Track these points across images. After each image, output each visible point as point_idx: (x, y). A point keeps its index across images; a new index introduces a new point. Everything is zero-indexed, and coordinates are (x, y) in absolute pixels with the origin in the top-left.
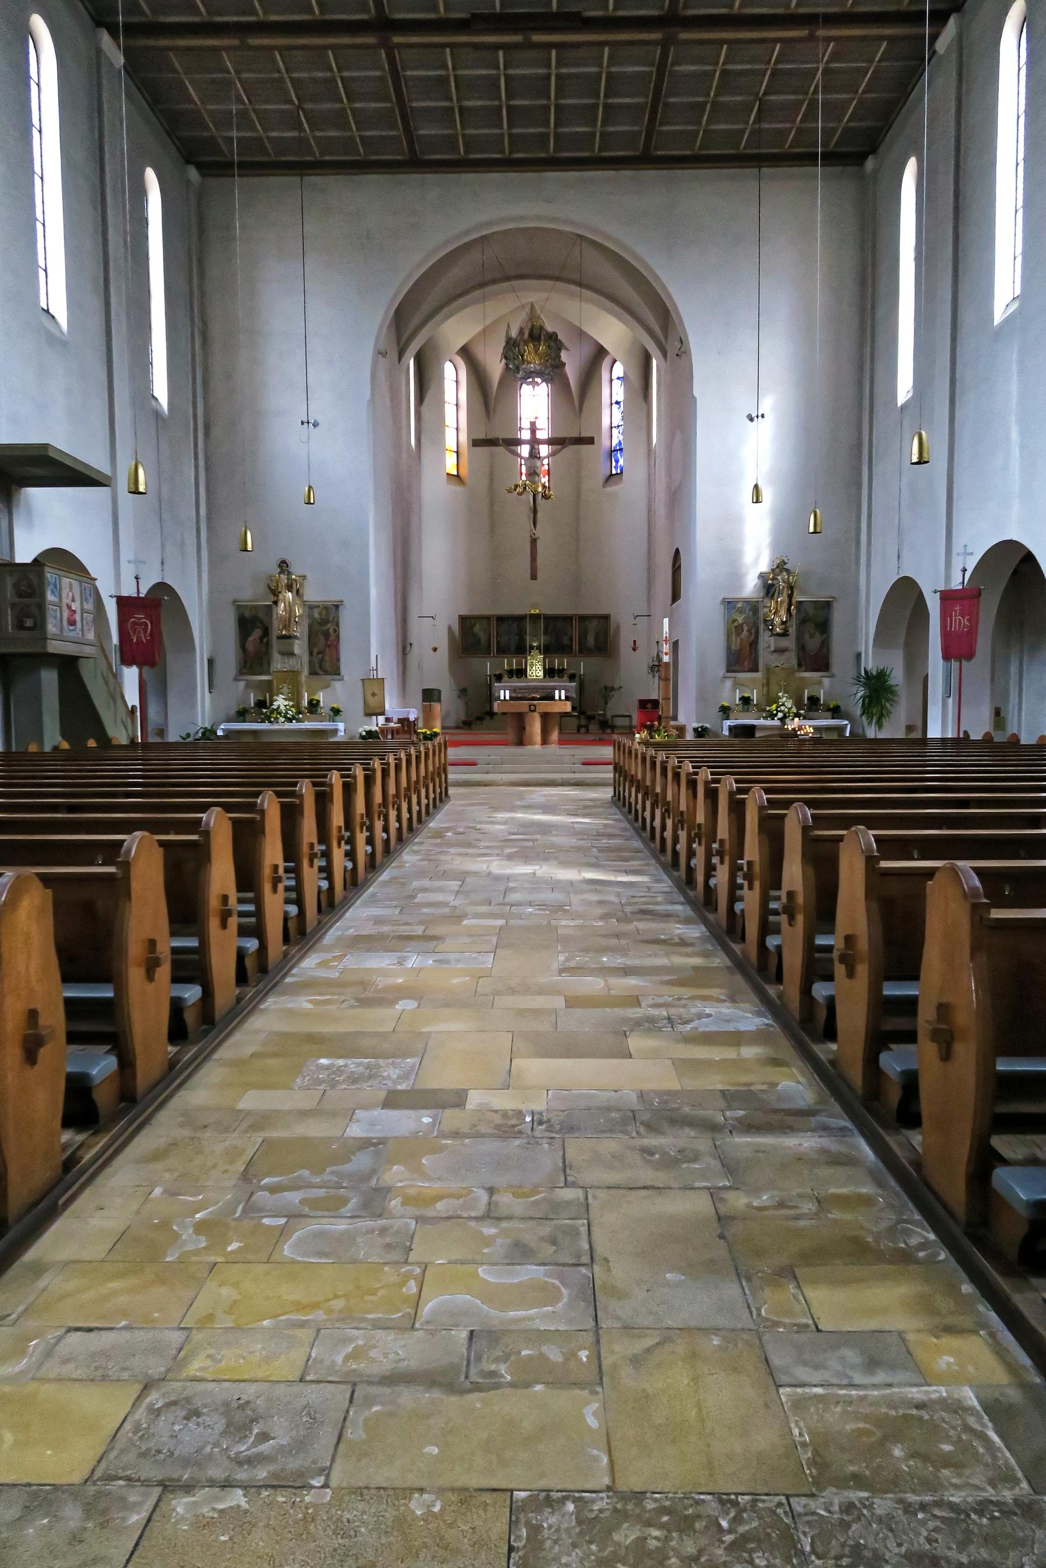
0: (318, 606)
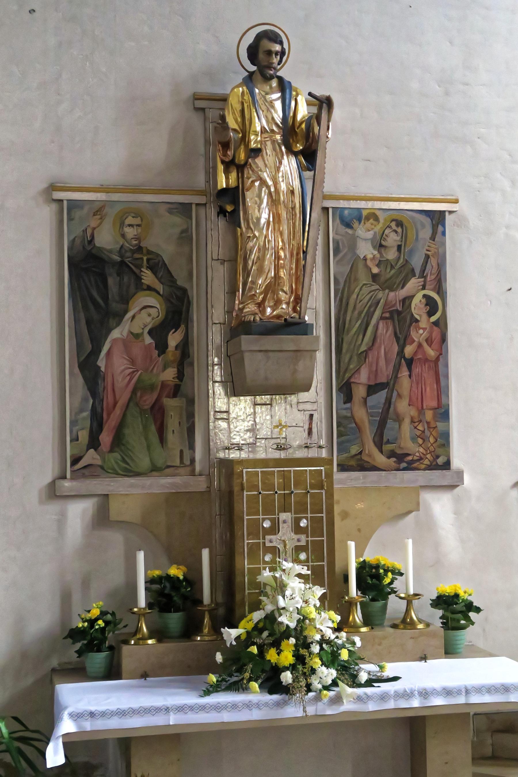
0: (373, 216)
